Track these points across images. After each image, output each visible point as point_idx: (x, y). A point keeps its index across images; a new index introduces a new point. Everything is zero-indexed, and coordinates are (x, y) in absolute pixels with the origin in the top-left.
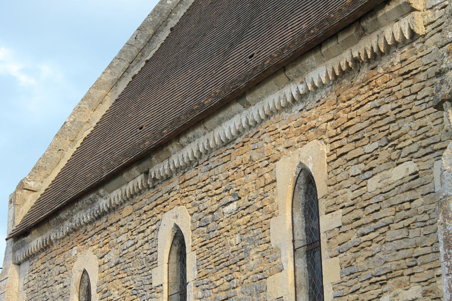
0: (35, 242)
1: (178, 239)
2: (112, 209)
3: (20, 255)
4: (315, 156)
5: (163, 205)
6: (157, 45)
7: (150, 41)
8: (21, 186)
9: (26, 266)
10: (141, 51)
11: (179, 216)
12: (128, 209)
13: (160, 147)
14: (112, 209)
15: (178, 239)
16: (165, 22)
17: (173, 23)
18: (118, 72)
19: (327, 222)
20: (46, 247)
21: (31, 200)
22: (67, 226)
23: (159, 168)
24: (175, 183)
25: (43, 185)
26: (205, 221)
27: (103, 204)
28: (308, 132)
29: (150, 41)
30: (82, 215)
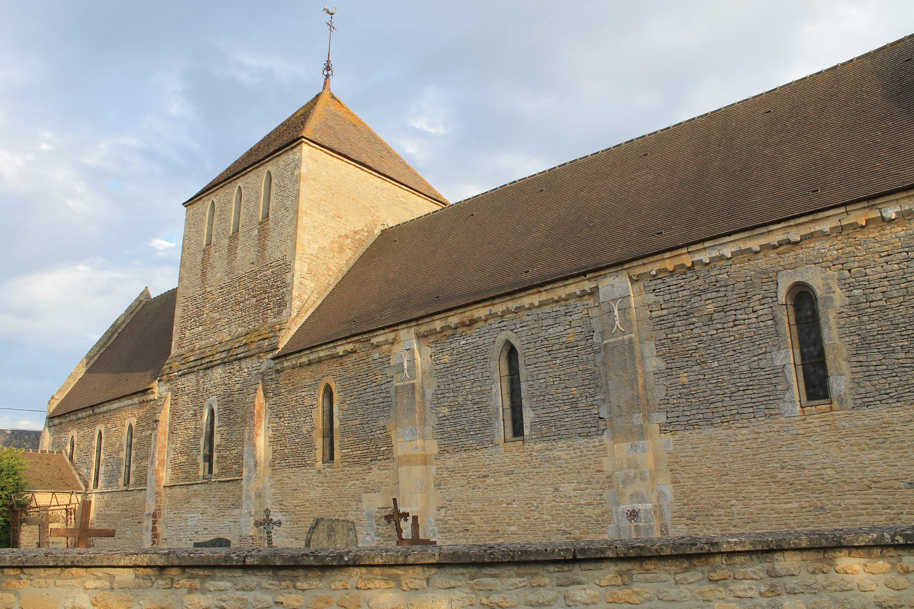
0: (57, 421)
1: (100, 433)
2: (83, 418)
3: (51, 424)
4: (134, 421)
5: (97, 422)
6: (112, 340)
7: (109, 338)
8: (53, 398)
9: (53, 428)
10: (105, 343)
11: (101, 427)
12: (87, 419)
13: (98, 405)
14: (83, 418)
15: (100, 433)
16: (116, 331)
17: (119, 331)
18: (95, 352)
19: (134, 441)
20: (60, 424)
21: (56, 403)
22: (68, 419)
23: (97, 410)
24: (101, 416)
25: (61, 397)
26: (107, 431)
27: (80, 415)
28: (134, 415)
29: (109, 338)
30: (73, 417)
